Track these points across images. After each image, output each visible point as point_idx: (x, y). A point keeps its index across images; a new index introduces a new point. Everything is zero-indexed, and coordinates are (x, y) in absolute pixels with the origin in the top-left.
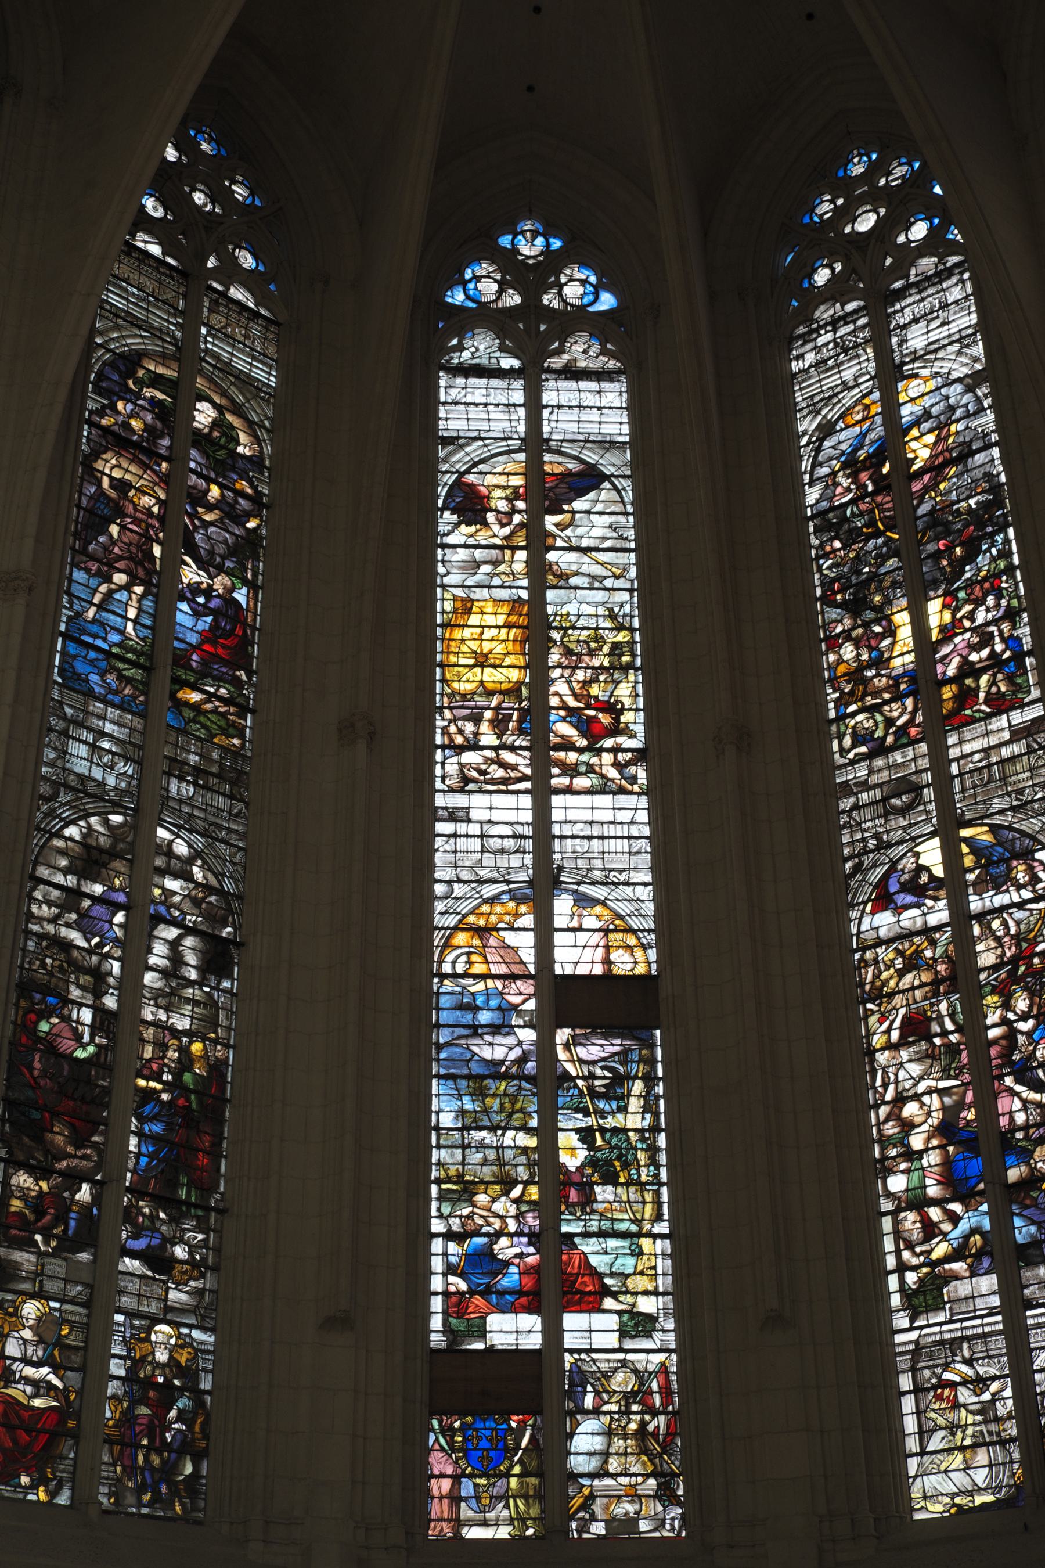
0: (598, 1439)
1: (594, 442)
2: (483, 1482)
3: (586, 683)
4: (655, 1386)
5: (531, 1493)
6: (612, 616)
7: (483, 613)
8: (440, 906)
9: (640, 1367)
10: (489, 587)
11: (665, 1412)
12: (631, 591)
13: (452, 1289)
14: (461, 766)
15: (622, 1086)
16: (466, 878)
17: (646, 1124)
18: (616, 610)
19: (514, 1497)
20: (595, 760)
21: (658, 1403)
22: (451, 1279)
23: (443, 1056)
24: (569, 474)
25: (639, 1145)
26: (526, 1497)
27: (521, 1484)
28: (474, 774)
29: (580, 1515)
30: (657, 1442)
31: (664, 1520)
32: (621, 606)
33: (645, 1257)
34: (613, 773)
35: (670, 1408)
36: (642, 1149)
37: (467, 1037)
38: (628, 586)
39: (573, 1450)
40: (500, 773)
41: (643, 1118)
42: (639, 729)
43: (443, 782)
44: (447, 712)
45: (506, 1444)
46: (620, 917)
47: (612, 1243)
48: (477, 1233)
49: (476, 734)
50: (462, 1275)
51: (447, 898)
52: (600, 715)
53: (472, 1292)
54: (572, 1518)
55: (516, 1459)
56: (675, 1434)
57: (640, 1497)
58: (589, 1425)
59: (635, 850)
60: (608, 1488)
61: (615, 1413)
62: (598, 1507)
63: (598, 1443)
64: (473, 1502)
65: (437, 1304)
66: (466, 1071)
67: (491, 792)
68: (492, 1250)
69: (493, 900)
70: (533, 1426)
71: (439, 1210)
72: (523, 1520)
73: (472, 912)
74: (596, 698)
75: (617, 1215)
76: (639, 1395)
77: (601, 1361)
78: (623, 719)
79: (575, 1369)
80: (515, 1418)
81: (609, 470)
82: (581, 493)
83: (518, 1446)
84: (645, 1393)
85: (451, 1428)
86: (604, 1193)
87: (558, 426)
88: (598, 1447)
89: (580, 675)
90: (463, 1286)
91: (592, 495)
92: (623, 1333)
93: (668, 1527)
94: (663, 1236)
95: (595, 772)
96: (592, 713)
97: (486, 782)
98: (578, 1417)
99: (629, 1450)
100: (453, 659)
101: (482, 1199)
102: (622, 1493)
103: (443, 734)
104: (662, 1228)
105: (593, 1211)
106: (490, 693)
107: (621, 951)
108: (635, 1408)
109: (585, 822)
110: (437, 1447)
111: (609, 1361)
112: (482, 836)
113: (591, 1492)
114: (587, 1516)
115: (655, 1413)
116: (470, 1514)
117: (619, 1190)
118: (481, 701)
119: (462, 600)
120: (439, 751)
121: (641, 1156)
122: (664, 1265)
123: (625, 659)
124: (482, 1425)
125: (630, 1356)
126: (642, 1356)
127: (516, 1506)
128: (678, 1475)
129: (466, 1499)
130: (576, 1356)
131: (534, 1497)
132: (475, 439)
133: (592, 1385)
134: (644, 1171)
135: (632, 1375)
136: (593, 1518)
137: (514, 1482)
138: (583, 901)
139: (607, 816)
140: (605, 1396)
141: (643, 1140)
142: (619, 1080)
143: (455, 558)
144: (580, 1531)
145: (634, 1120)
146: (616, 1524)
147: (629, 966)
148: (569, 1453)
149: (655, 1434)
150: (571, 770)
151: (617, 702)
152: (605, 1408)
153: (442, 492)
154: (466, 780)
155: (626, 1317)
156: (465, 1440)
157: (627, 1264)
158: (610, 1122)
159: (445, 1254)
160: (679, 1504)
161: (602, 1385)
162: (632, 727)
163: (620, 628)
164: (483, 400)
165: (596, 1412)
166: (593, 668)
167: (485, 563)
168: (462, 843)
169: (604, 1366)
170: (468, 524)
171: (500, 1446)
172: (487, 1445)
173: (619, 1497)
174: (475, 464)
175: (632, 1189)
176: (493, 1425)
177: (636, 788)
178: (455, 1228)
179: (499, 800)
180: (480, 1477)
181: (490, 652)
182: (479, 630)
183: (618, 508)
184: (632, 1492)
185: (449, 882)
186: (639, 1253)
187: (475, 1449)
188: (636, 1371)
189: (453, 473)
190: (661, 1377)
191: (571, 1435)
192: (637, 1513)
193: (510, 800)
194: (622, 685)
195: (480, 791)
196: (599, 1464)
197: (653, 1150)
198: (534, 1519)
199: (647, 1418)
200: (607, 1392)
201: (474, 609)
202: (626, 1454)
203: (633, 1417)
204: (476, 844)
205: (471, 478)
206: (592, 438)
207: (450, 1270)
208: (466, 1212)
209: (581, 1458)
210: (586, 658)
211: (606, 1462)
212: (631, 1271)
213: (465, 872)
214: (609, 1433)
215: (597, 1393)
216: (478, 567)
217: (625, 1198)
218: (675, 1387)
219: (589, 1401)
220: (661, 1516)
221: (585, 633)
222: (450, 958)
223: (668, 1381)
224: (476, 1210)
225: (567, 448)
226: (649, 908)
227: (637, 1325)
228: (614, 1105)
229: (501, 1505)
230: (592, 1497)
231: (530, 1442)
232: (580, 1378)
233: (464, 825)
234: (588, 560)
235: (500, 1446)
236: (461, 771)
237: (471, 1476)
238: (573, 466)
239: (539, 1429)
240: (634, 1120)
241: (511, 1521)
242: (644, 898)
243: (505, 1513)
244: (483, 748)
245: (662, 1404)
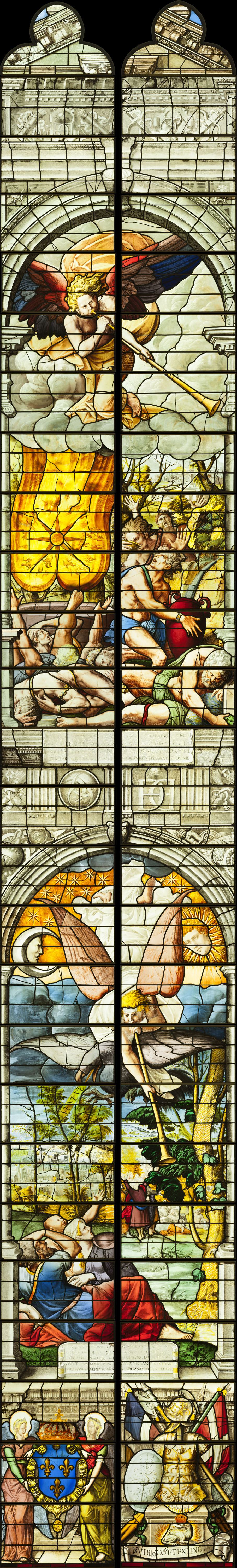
1: (188, 195)
3: (167, 573)
4: (211, 1417)
6: (202, 475)
7: (58, 472)
8: (9, 877)
10: (66, 433)
12: (225, 434)
13: (24, 1316)
14: (34, 692)
15: (190, 1091)
16: (38, 841)
17: (215, 1135)
18: (207, 464)
20: (174, 682)
22: (23, 1307)
23: (13, 1060)
24: (157, 251)
25: (206, 1160)
28: (49, 703)
32: (214, 459)
33: (208, 1283)
34: (195, 701)
35: (226, 1438)
36: (209, 1164)
37: (39, 1038)
38: (223, 427)
40: (74, 700)
41: (212, 1129)
42: (227, 635)
43: (12, 714)
44: (16, 618)
46: (196, 888)
47: (176, 1268)
48: (47, 1258)
49: (51, 647)
50: (35, 1303)
51: (17, 867)
52: (183, 619)
53: (44, 1321)
58: (144, 1455)
59: (215, 803)
65: (9, 1331)
66: (38, 1079)
67: (67, 727)
68: (65, 1276)
69: (67, 869)
71: (10, 1233)
73: (44, 884)
74: (177, 593)
75: (181, 1238)
76: (197, 1424)
78: (209, 623)
81: (205, 242)
82: (170, 282)
85: (24, 1457)
86: (167, 1213)
87: (149, 166)
89: (161, 562)
90: (36, 1315)
91: (183, 286)
92: (182, 1364)
93: (216, 1553)
94: (227, 1261)
95: (174, 699)
96: (173, 615)
97: (62, 714)
100: (23, 544)
101: (54, 1222)
102: (174, 1520)
103: (11, 649)
104: (226, 1251)
105: (156, 1234)
106: (67, 589)
107: (195, 932)
108: (191, 1437)
109: (161, 766)
110: (10, 1475)
112: (57, 786)
115: (210, 1443)
117: (185, 1210)
118: (55, 600)
119: (34, 452)
120: (6, 674)
121: (208, 1171)
122: (227, 1291)
123: (216, 536)
125: (188, 1386)
132: (49, 195)
134: (210, 1188)
135: (188, 1404)
138: (158, 869)
139: (184, 757)
141: (212, 1153)
142: (188, 1085)
143: (25, 388)
144: (131, 1557)
145: (203, 1132)
147: (203, 951)
150: (146, 697)
151: (203, 599)
152: (161, 1438)
153: (9, 283)
154: (39, 711)
155: (185, 1347)
157: (189, 1289)
158: (176, 1135)
159: (17, 1280)
160: (228, 1531)
162: (220, 634)
163: (212, 491)
164: (59, 129)
166: (176, 551)
167: (62, 395)
168: (34, 796)
170: (41, 336)
172: (60, 1474)
174: (50, 239)
175: (197, 1209)
177: (219, 720)
178: (27, 1254)
179: (75, 736)
181: (69, 529)
182: (54, 498)
183: (216, 303)
184: (184, 1520)
185: (20, 846)
186: (202, 1279)
188: (192, 1402)
189: (21, 253)
193: (89, 736)
194: (210, 575)
195: (55, 727)
197: (220, 1164)
199: (202, 1447)
200: (164, 1422)
201: (48, 467)
204: (48, 796)
205: (45, 261)
206: (186, 188)
207: (21, 1297)
208: (36, 1235)
210: (168, 537)
212: (193, 1298)
213: (37, 833)
216: (54, 401)
217: (189, 1219)
221: (168, 499)
222: (21, 941)
223: (224, 1411)
224: (48, 1233)
225: (154, 207)
226: (229, 874)
227: (196, 1354)
228: (182, 1113)
233: (37, 772)
234: (175, 388)
235: (71, 1475)
236: (34, 700)
238: (162, 237)
240: (203, 1132)
242: (224, 863)
244: (58, 669)
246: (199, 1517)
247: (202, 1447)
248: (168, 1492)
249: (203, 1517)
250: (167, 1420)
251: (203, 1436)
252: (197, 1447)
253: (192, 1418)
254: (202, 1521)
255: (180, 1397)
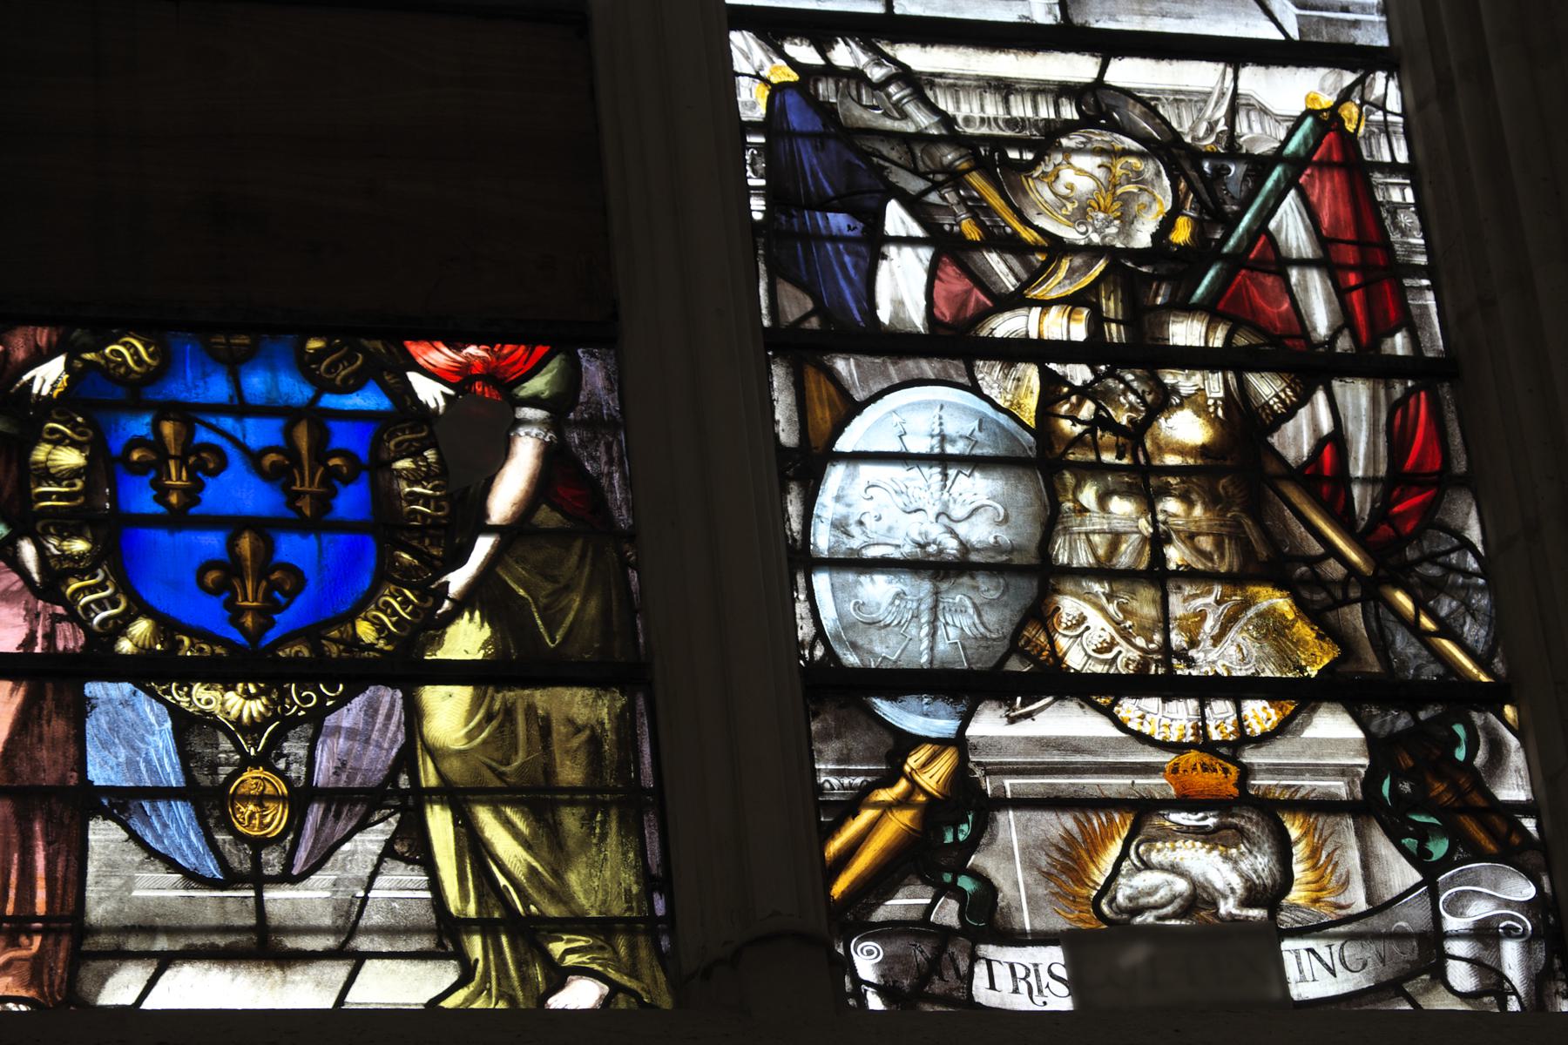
0: (977, 488)
2: (239, 704)
5: (570, 773)
9: (1184, 123)
11: (1368, 363)
19: (459, 800)
21: (1321, 319)
26: (536, 799)
27: (497, 725)
29: (903, 903)
30: (1344, 519)
31: (1432, 942)
39: (823, 540)
45: (384, 499)
54: (854, 917)
55: (457, 580)
56: (1443, 482)
57: (1271, 810)
60: (1065, 756)
61: (1067, 351)
62: (1011, 858)
63: (981, 510)
64: (177, 826)
70: (558, 407)
72: (530, 934)
77: (957, 85)
79: (799, 118)
80: (440, 356)
83: (467, 514)
84: (1236, 262)
88: (981, 532)
98: (844, 366)
99: (1175, 555)
102: (1156, 785)
108: (1186, 332)
111: (1004, 88)
113: (961, 778)
114: (948, 913)
115: (1311, 368)
116: (156, 889)
124: (218, 389)
125: (1127, 73)
126: (1202, 75)
127: (473, 846)
128: (1491, 698)
129: (122, 803)
130: (805, 53)
131: (591, 798)
133: (914, 205)
135: (1149, 168)
136: (988, 922)
137: (448, 713)
140: (1002, 269)
146: (1136, 955)
148: (806, 560)
149: (1325, 471)
152: (1006, 325)
156: (105, 464)
161: (978, 209)
165: (953, 344)
169: (976, 113)
171: (348, 502)
173: (1143, 810)
176: (295, 390)
180: (223, 675)
184: (1221, 780)
187: (179, 520)
190: (1326, 190)
191: (810, 463)
192: (1268, 894)
196: (997, 621)
198: (601, 928)
199: (1267, 388)
202: (1157, 576)
203: (1184, 381)
209: (878, 590)
211: (1040, 613)
214: (1040, 462)
215: (948, 249)
218: (1411, 239)
219: (903, 285)
220: (1413, 917)
229: (371, 841)
230: (968, 802)
231: (542, 488)
232: (839, 165)
237: (147, 672)
239: (595, 424)
241: (443, 935)
243: (399, 887)
245: (1344, 320)
246: (1317, 771)
247: (1267, 388)
248: (1095, 619)
249: (1343, 771)
250: (1028, 235)
251: (1257, 329)
252: (1243, 385)
253: (1182, 233)
254: (1339, 788)
255: (1086, 122)
